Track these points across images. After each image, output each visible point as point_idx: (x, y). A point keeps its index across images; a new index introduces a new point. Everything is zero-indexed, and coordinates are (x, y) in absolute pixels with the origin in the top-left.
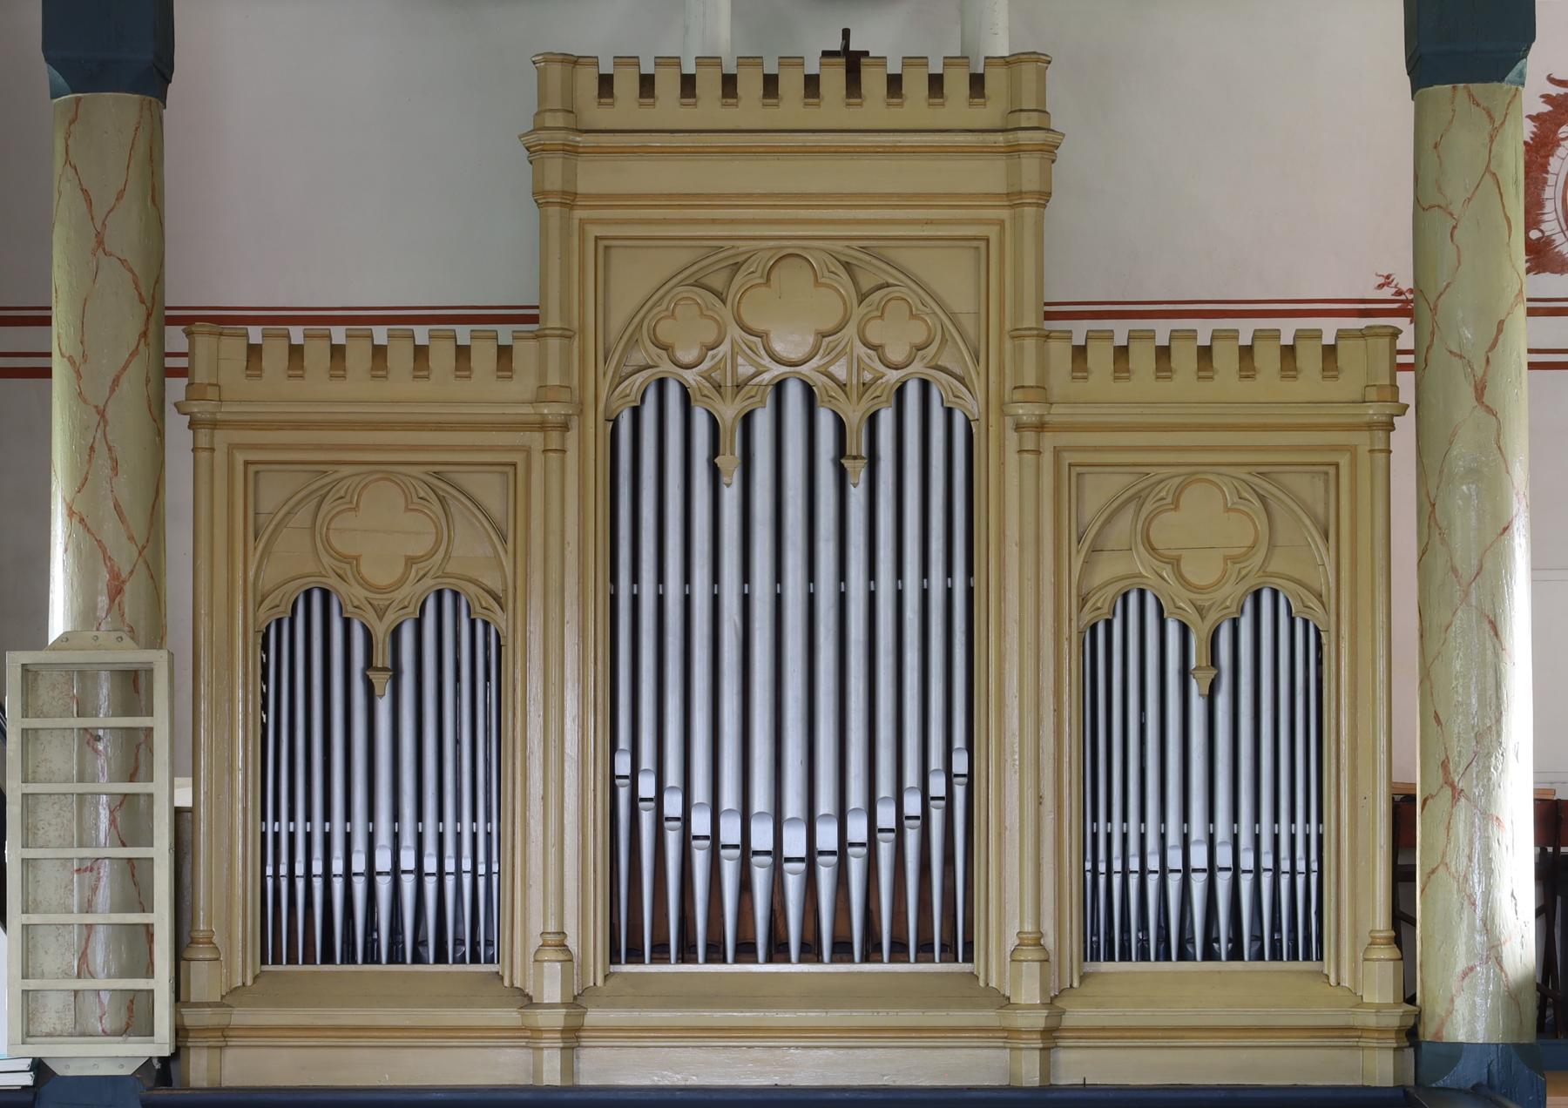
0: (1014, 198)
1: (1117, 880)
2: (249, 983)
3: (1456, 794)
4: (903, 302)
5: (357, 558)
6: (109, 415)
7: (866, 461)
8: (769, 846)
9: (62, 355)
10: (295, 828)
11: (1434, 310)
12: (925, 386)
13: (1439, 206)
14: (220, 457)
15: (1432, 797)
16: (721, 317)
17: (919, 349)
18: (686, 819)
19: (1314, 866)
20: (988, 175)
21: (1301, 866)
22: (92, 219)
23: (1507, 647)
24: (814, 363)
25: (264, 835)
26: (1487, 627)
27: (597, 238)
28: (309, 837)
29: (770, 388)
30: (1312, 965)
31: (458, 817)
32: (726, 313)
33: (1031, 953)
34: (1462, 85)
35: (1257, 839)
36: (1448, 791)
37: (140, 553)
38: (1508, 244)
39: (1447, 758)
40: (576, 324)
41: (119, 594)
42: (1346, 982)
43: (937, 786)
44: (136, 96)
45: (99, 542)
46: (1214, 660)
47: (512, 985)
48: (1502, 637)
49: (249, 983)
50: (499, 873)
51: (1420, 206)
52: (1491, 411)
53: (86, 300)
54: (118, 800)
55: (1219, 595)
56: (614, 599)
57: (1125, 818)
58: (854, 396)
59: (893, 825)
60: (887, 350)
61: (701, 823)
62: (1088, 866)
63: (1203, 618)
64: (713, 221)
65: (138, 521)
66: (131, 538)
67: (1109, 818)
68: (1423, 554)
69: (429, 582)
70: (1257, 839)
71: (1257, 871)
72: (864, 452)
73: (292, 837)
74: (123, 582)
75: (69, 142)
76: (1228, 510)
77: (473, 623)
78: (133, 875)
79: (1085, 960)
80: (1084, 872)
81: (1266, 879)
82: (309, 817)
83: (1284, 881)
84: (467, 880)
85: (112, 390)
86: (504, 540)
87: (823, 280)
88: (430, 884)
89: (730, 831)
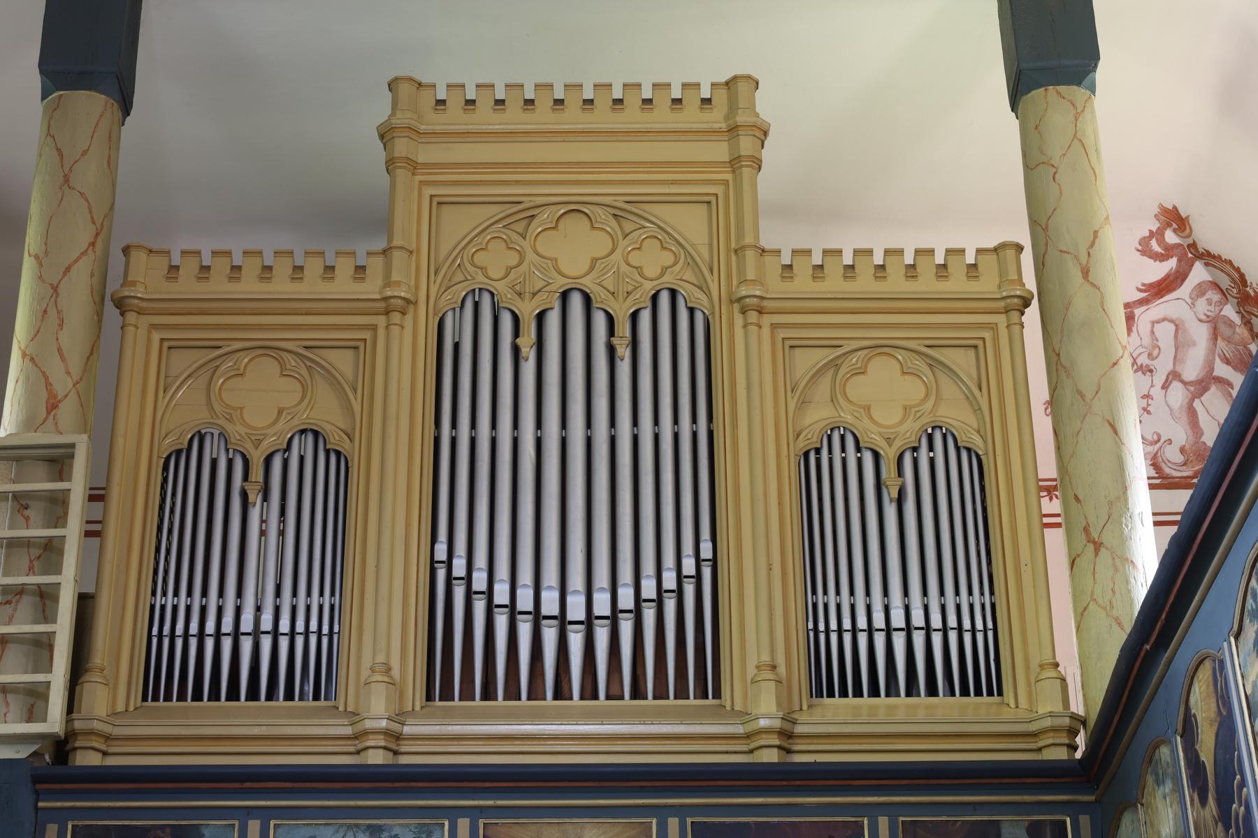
0: (735, 163)
1: (834, 637)
2: (131, 709)
3: (1098, 546)
4: (655, 240)
5: (242, 409)
6: (62, 289)
7: (630, 339)
8: (555, 611)
9: (30, 256)
10: (178, 601)
11: (1046, 229)
12: (673, 293)
13: (1043, 163)
14: (142, 332)
15: (1079, 556)
16: (521, 247)
18: (490, 593)
19: (990, 625)
20: (719, 151)
21: (979, 626)
22: (62, 166)
23: (1125, 442)
25: (152, 607)
26: (1109, 429)
27: (432, 196)
28: (188, 609)
29: (558, 294)
30: (996, 699)
31: (309, 594)
32: (526, 245)
33: (769, 675)
34: (1052, 87)
35: (943, 608)
36: (1091, 547)
37: (74, 385)
38: (1095, 185)
39: (1087, 523)
40: (414, 246)
41: (55, 408)
42: (1023, 703)
44: (103, 96)
45: (43, 373)
47: (346, 710)
48: (1121, 434)
49: (131, 709)
50: (339, 633)
51: (1028, 168)
52: (1093, 285)
53: (51, 217)
54: (35, 552)
55: (902, 429)
56: (437, 441)
57: (838, 593)
58: (621, 299)
59: (654, 596)
60: (644, 270)
61: (501, 594)
62: (811, 626)
63: (890, 446)
64: (517, 182)
66: (68, 373)
67: (825, 592)
69: (296, 422)
70: (943, 608)
71: (945, 630)
72: (628, 333)
74: (60, 401)
76: (904, 373)
77: (327, 452)
78: (44, 611)
79: (812, 696)
81: (953, 636)
83: (967, 638)
85: (65, 274)
87: (596, 225)
88: (284, 643)
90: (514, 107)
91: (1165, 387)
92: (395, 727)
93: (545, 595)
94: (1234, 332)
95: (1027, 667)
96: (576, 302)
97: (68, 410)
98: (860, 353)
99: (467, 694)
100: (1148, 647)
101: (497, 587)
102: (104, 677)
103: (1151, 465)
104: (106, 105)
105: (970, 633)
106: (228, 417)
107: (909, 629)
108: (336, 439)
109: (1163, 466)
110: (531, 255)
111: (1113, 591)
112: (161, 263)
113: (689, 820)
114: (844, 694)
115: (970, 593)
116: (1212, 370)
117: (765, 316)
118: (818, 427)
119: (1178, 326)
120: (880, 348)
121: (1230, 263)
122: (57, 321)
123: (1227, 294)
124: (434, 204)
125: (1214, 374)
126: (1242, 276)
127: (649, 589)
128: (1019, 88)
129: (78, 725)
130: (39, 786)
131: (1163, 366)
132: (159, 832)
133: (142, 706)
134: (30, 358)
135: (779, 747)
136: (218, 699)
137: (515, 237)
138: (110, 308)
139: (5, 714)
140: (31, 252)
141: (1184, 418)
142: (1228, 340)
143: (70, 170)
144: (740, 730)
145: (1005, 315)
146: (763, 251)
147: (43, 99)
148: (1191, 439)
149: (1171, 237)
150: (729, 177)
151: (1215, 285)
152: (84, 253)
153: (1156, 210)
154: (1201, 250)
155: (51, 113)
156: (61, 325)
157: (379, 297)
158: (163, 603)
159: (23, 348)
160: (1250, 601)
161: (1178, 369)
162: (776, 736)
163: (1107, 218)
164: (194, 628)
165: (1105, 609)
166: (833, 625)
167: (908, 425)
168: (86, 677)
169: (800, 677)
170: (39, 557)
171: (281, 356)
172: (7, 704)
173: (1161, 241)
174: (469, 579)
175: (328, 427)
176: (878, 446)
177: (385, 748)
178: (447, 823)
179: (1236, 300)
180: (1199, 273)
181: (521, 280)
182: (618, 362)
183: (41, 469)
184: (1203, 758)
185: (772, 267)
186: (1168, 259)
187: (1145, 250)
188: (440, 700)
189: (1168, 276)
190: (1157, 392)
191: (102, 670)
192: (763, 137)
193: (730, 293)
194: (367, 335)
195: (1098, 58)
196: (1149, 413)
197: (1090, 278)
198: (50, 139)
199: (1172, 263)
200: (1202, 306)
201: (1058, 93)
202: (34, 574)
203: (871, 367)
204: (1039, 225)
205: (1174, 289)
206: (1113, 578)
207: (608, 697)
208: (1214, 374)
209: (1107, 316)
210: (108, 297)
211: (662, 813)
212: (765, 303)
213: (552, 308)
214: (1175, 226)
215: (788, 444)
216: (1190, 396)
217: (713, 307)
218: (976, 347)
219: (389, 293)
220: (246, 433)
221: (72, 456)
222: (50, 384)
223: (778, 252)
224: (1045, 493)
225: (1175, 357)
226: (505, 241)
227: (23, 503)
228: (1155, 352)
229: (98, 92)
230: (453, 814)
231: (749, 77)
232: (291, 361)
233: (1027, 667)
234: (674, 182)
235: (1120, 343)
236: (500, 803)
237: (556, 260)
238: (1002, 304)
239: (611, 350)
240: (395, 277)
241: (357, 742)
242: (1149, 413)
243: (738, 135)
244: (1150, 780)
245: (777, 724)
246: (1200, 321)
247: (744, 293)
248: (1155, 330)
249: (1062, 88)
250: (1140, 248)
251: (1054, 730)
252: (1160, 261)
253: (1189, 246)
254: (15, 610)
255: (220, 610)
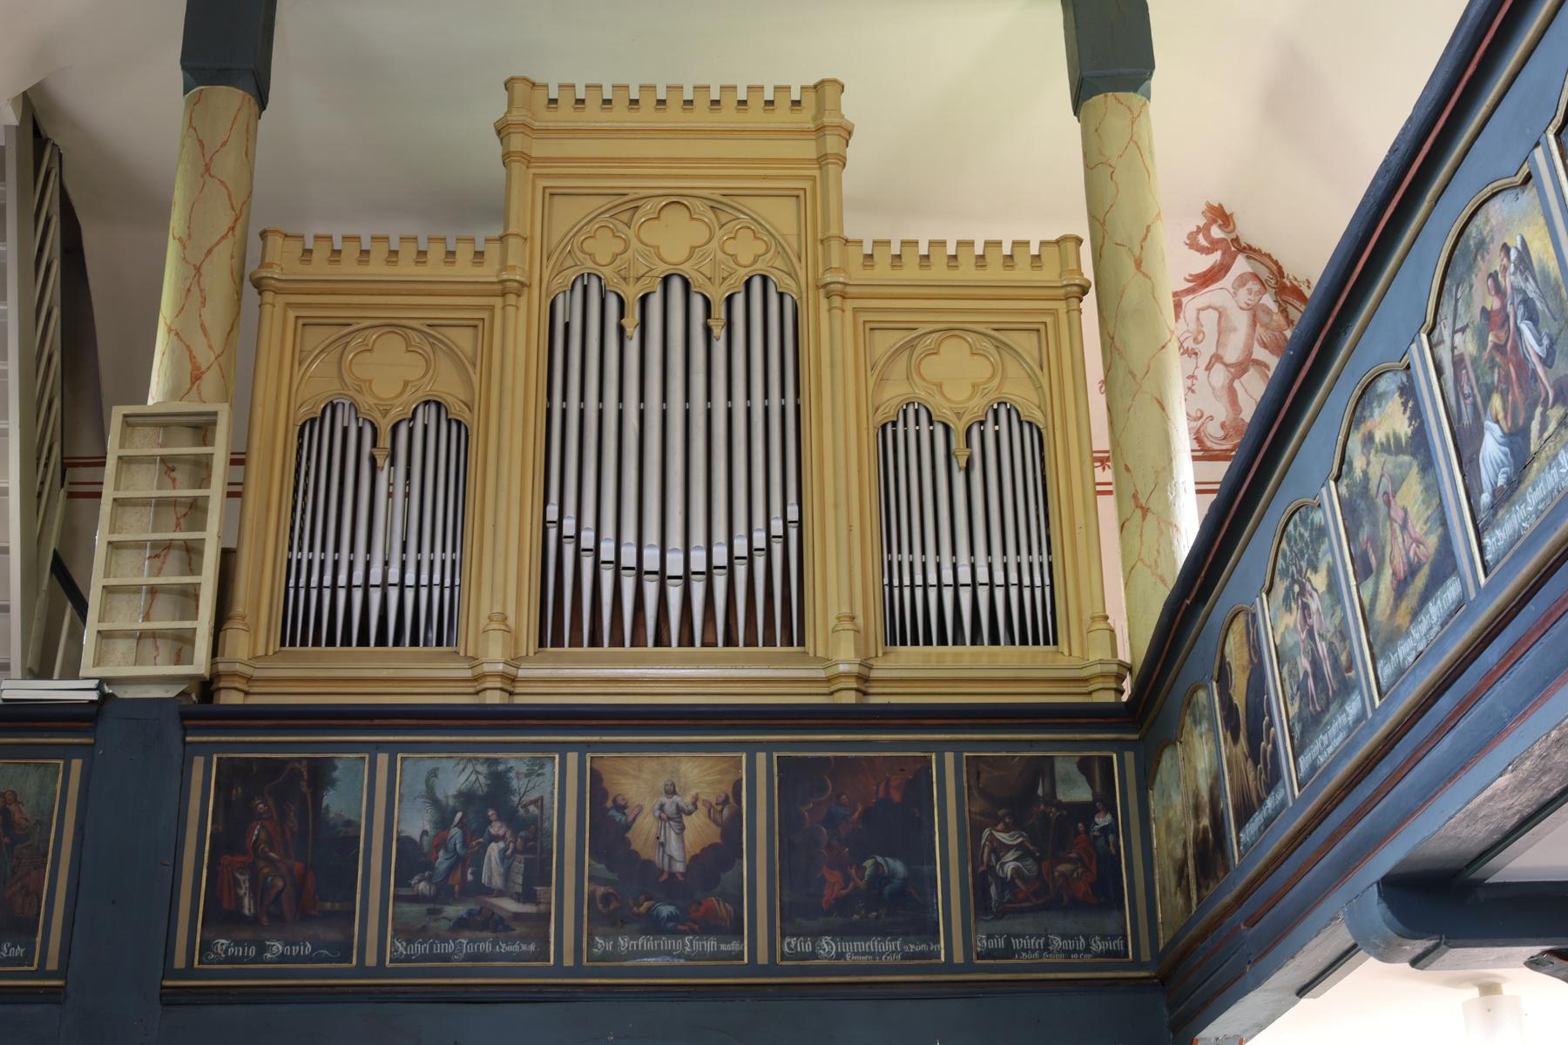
0: (822, 160)
1: (907, 592)
2: (271, 653)
3: (1145, 511)
4: (749, 231)
5: (370, 381)
6: (203, 270)
7: (725, 321)
8: (656, 567)
9: (174, 239)
10: (313, 556)
11: (1103, 224)
12: (765, 279)
14: (278, 311)
15: (1128, 520)
17: (759, 256)
18: (597, 550)
19: (1047, 581)
20: (808, 149)
21: (1038, 582)
22: (204, 156)
24: (692, 261)
25: (289, 561)
26: (1156, 405)
27: (544, 188)
28: (322, 563)
30: (1051, 648)
32: (631, 233)
33: (848, 625)
34: (1110, 94)
36: (1139, 513)
37: (216, 359)
39: (1136, 490)
40: (528, 234)
41: (199, 379)
43: (777, 526)
44: (241, 92)
45: (188, 347)
46: (968, 444)
49: (271, 653)
50: (460, 585)
51: (1088, 167)
52: (1145, 275)
54: (182, 510)
55: (970, 404)
59: (745, 554)
61: (607, 552)
62: (886, 581)
63: (960, 419)
64: (623, 176)
65: (217, 339)
66: (211, 347)
67: (900, 551)
68: (1108, 371)
69: (420, 393)
71: (1007, 586)
72: (723, 315)
73: (310, 562)
74: (203, 373)
75: (193, 115)
77: (449, 421)
78: (190, 564)
79: (886, 645)
80: (883, 586)
81: (1014, 591)
82: (323, 549)
83: (1027, 593)
84: (436, 591)
85: (206, 256)
86: (474, 366)
88: (409, 595)
89: (628, 558)
90: (620, 106)
91: (1208, 368)
92: (511, 670)
93: (646, 552)
94: (1272, 319)
95: (1080, 620)
96: (676, 287)
97: (210, 381)
98: (934, 335)
99: (576, 641)
100: (1188, 602)
101: (603, 545)
102: (246, 624)
103: (1195, 439)
104: (244, 100)
105: (1029, 589)
106: (358, 389)
107: (974, 585)
108: (458, 410)
109: (1205, 440)
110: (635, 243)
111: (1158, 552)
112: (296, 248)
113: (775, 755)
114: (915, 642)
115: (1030, 553)
116: (1251, 353)
117: (849, 301)
118: (895, 402)
119: (1221, 313)
120: (952, 331)
121: (1269, 256)
122: (200, 299)
123: (1266, 286)
124: (547, 196)
125: (1253, 357)
126: (1280, 269)
127: (741, 548)
128: (1081, 93)
129: (221, 667)
130: (187, 723)
131: (1207, 349)
132: (296, 764)
133: (280, 651)
134: (176, 333)
135: (857, 690)
136: (350, 645)
137: (621, 226)
138: (248, 287)
139: (155, 658)
140: (175, 235)
141: (1225, 398)
142: (1266, 326)
143: (211, 158)
144: (822, 674)
145: (1064, 302)
146: (847, 241)
147: (185, 93)
148: (1231, 415)
149: (1216, 232)
150: (816, 173)
151: (1256, 276)
152: (224, 237)
153: (1204, 207)
154: (1243, 244)
155: (193, 107)
156: (203, 303)
157: (496, 280)
158: (299, 557)
159: (168, 323)
160: (1280, 561)
161: (1221, 352)
162: (854, 680)
163: (1159, 214)
164: (327, 580)
165: (1150, 567)
166: (907, 581)
167: (976, 401)
168: (229, 625)
169: (876, 627)
170: (185, 515)
171: (407, 334)
172: (157, 648)
173: (1208, 236)
174: (577, 537)
175: (449, 399)
176: (948, 419)
177: (502, 689)
178: (557, 756)
179: (1274, 290)
180: (1241, 265)
181: (626, 265)
182: (714, 342)
183: (187, 434)
184: (1236, 701)
185: (855, 256)
186: (1213, 252)
187: (1193, 244)
188: (552, 646)
189: (1212, 268)
190: (1201, 373)
191: (244, 618)
192: (848, 137)
193: (816, 279)
194: (485, 315)
195: (1154, 67)
196: (1193, 392)
197: (1142, 269)
198: (192, 130)
199: (1216, 256)
200: (1243, 295)
201: (1116, 99)
202: (181, 530)
203: (943, 348)
204: (1098, 220)
205: (1218, 280)
206: (1158, 541)
207: (703, 645)
208: (1253, 357)
209: (1157, 303)
210: (247, 278)
211: (752, 748)
212: (849, 290)
213: (654, 292)
214: (1220, 222)
215: (868, 417)
216: (1231, 377)
217: (801, 292)
218: (1038, 330)
219: (505, 277)
220: (375, 404)
221: (215, 423)
222: (194, 357)
223: (860, 243)
224: (1099, 464)
225: (1218, 341)
226: (612, 230)
227: (170, 465)
228: (1200, 337)
229: (236, 87)
230: (563, 748)
231: (835, 81)
232: (415, 338)
233: (1080, 620)
234: (765, 177)
235: (1169, 328)
236: (605, 738)
237: (658, 248)
238: (1062, 292)
239: (708, 331)
240: (511, 262)
241: (476, 684)
242: (1193, 392)
243: (825, 135)
244: (1188, 720)
245: (855, 669)
246: (1241, 308)
247: (829, 280)
248: (1200, 316)
249: (1119, 95)
250: (1188, 242)
251: (1103, 676)
252: (1206, 254)
253: (1232, 240)
254: (164, 563)
255: (351, 564)
